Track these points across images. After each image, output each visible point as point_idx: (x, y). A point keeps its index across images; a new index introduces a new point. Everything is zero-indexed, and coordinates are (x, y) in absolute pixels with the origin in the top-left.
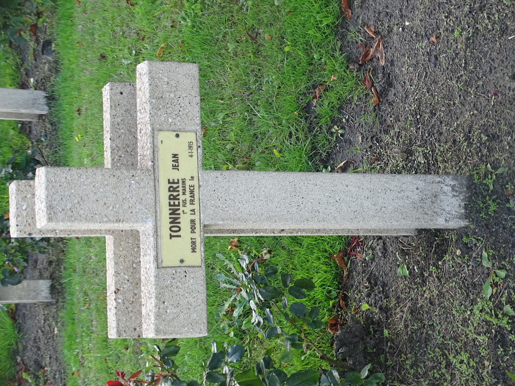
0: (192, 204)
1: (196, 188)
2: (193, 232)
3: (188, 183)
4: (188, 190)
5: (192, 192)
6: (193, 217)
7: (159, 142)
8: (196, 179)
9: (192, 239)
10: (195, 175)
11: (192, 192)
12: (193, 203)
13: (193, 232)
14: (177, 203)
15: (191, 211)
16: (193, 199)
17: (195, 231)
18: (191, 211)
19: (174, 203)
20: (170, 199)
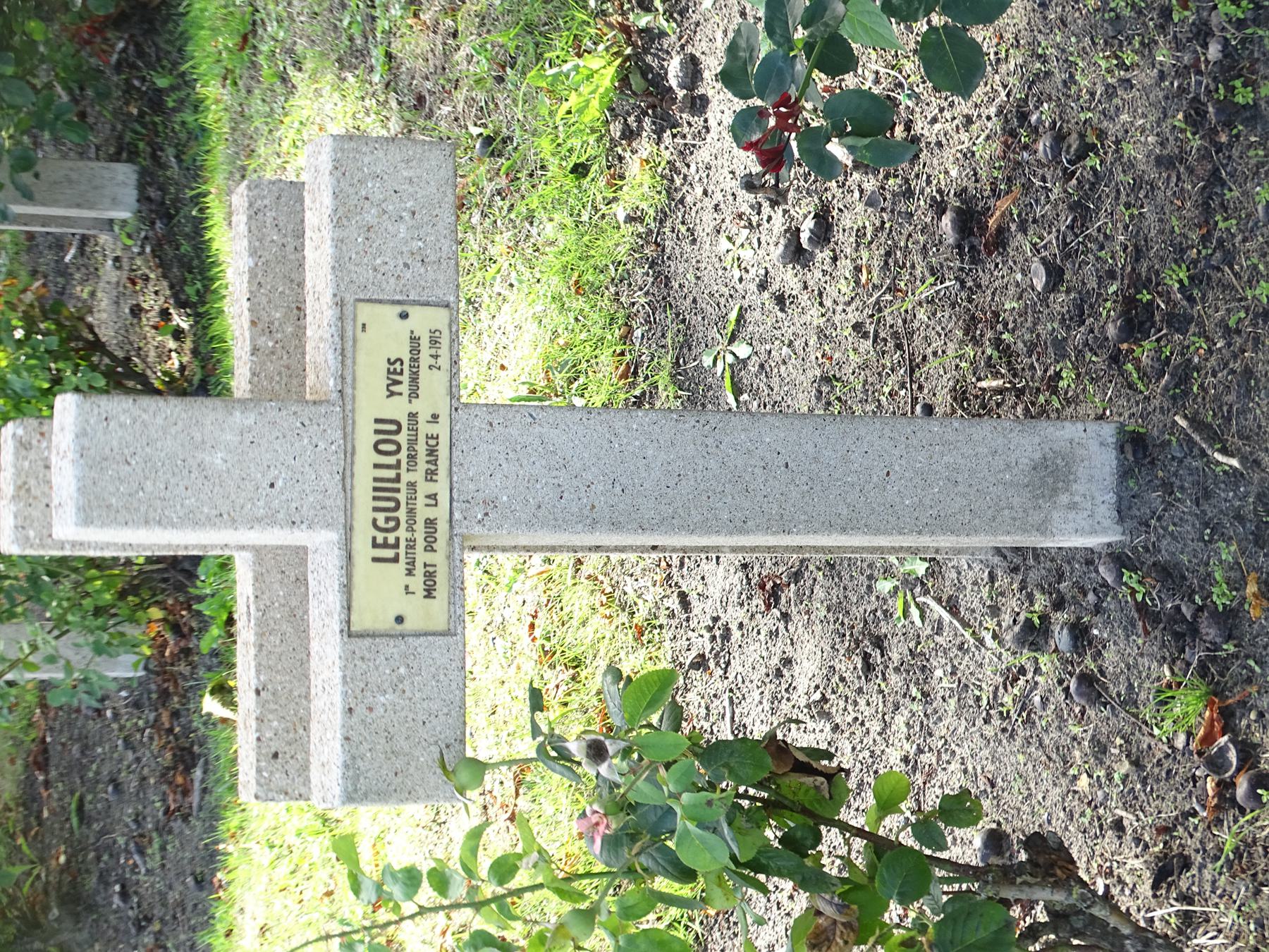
0: (431, 480)
1: (440, 440)
2: (429, 548)
3: (424, 429)
4: (421, 448)
5: (432, 452)
6: (431, 513)
8: (444, 419)
11: (432, 452)
12: (435, 477)
13: (429, 548)
14: (391, 540)
15: (428, 497)
16: (433, 468)
18: (428, 497)
19: (386, 539)
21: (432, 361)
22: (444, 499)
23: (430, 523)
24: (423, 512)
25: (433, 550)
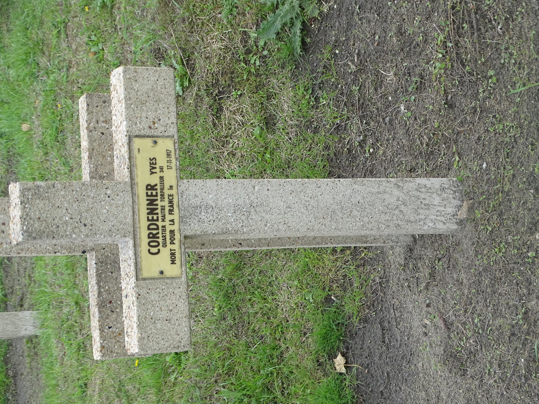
0: (171, 214)
2: (172, 243)
3: (167, 192)
4: (166, 199)
5: (171, 202)
6: (172, 228)
7: (136, 151)
9: (171, 250)
10: (174, 184)
11: (171, 202)
12: (173, 213)
15: (170, 221)
16: (172, 208)
17: (174, 242)
18: (170, 221)
20: (149, 237)
21: (168, 164)
22: (176, 221)
23: (172, 232)
24: (169, 228)
25: (174, 244)
